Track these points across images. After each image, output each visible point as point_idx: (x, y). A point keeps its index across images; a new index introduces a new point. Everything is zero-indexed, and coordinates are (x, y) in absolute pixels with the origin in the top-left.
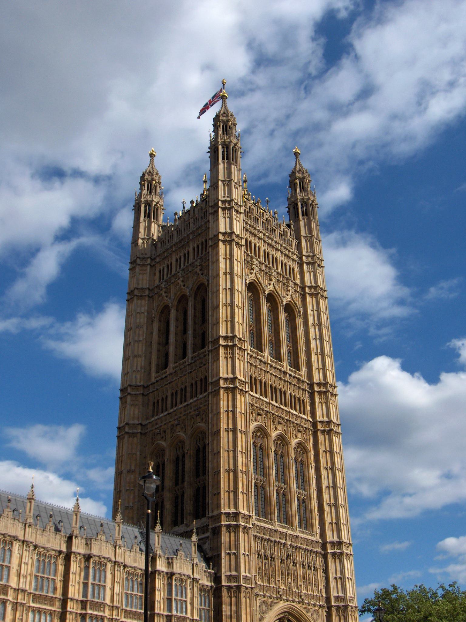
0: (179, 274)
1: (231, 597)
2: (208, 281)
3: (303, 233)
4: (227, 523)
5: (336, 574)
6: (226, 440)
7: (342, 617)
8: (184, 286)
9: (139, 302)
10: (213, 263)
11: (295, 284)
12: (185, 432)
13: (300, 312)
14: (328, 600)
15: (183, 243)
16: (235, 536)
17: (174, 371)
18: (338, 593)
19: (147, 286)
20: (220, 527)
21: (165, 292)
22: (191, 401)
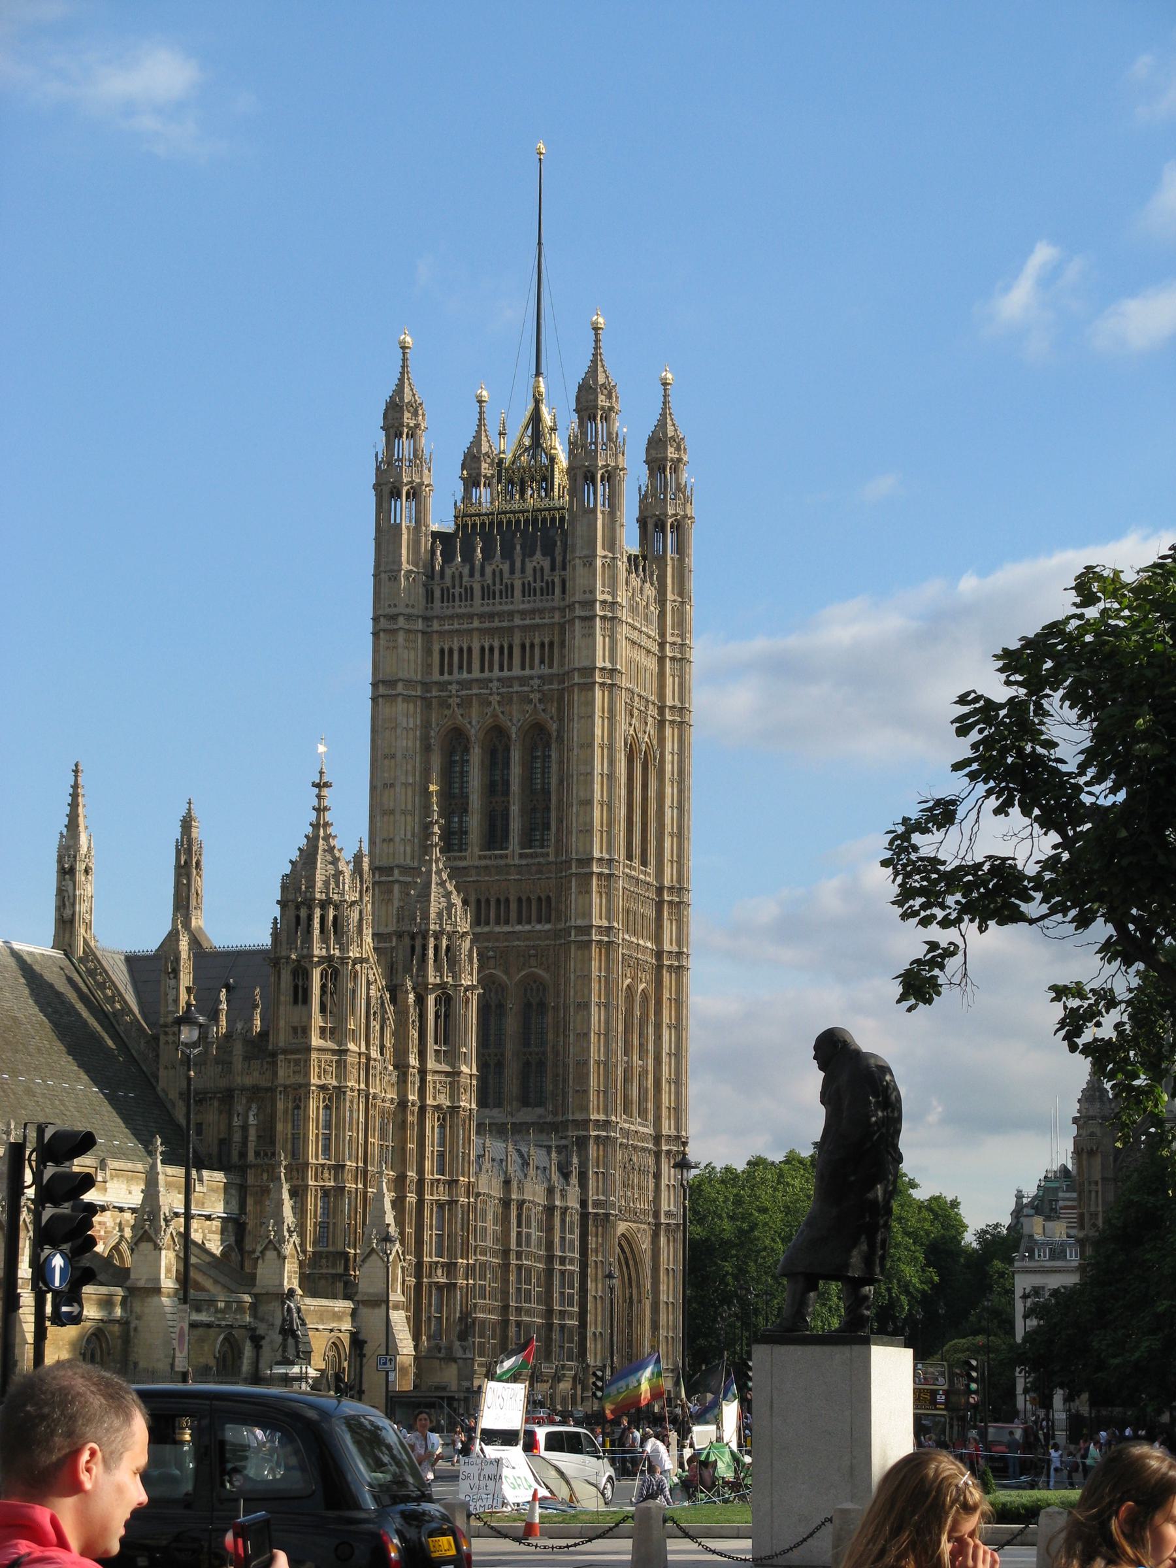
0: (490, 685)
1: (597, 1227)
2: (560, 731)
3: (670, 596)
4: (596, 1133)
5: (669, 1181)
6: (597, 1018)
7: (671, 1238)
8: (503, 713)
9: (405, 705)
10: (580, 718)
11: (654, 704)
12: (506, 972)
13: (655, 758)
14: (656, 1214)
15: (496, 624)
16: (604, 1151)
17: (484, 863)
18: (669, 1206)
19: (419, 677)
20: (587, 1137)
21: (458, 704)
22: (519, 928)
